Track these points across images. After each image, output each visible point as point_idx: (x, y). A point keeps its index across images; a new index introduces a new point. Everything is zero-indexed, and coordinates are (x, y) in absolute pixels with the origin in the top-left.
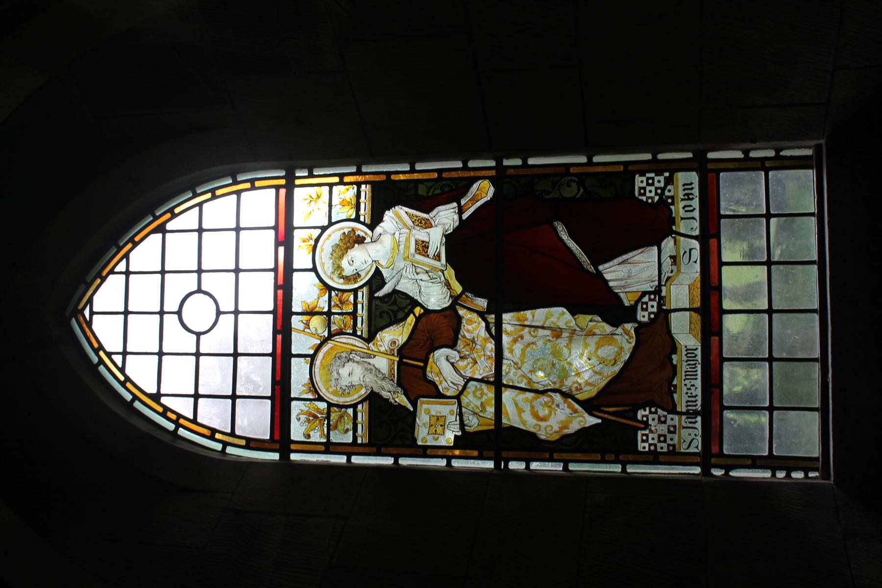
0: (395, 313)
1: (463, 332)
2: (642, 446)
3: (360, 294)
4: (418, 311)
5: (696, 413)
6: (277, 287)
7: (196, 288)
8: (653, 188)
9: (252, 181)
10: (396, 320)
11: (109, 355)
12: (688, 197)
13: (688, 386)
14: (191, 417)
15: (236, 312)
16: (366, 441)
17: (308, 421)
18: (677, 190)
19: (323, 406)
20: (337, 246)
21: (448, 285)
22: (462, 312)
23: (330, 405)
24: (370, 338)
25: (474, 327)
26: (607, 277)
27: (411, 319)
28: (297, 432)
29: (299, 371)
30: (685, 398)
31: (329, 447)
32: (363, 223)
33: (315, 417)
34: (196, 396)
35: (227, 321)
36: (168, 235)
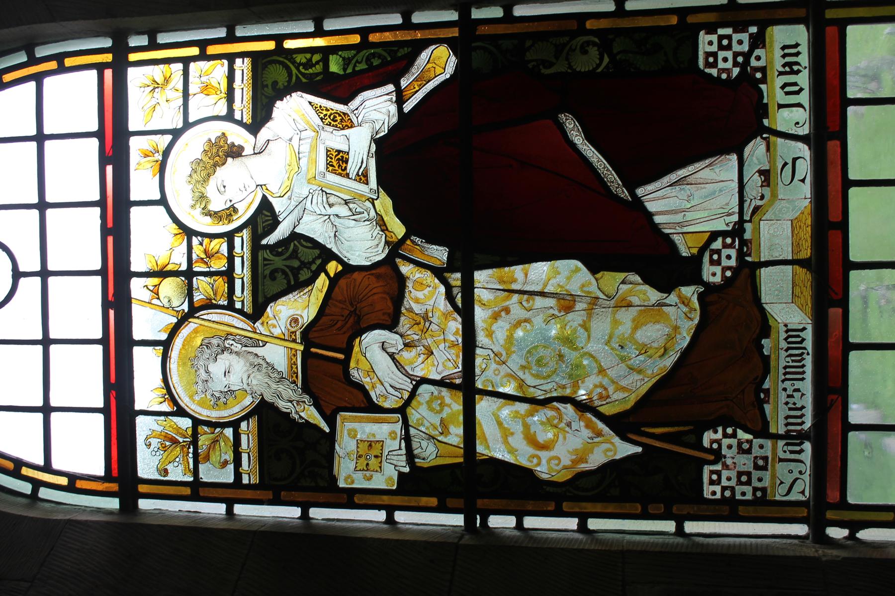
0: (296, 272)
1: (409, 302)
2: (709, 491)
3: (237, 241)
4: (333, 267)
5: (802, 436)
6: (105, 231)
8: (729, 54)
9: (60, 58)
10: (297, 283)
12: (791, 68)
13: (789, 392)
15: (44, 274)
16: (255, 480)
17: (165, 448)
18: (771, 57)
19: (185, 423)
20: (199, 161)
21: (381, 224)
22: (406, 269)
23: (197, 422)
24: (256, 314)
25: (425, 294)
26: (651, 207)
27: (322, 282)
28: (147, 465)
29: (146, 364)
30: (783, 411)
31: (197, 490)
32: (240, 123)
33: (174, 442)
35: (30, 287)
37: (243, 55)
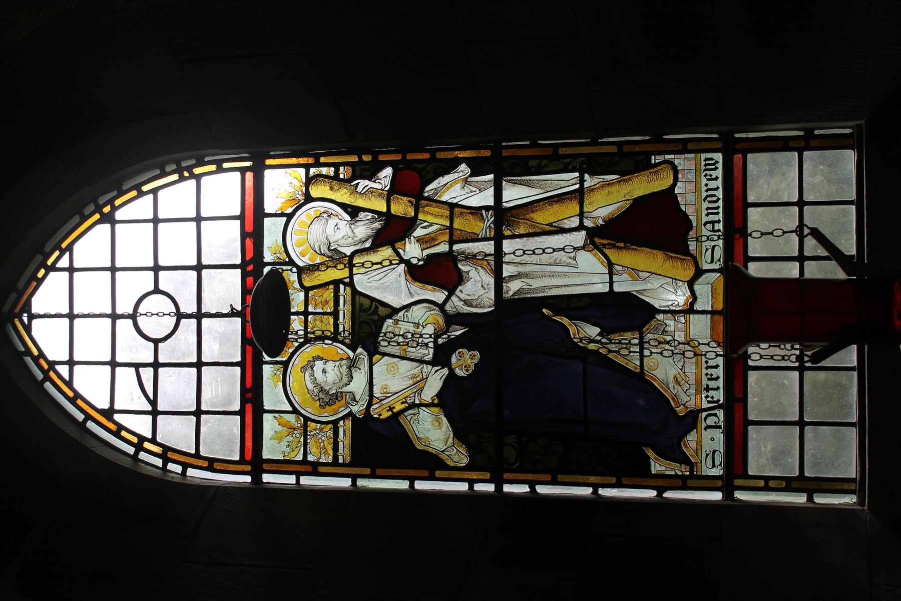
7: (152, 288)
11: (52, 364)
36: (118, 226)
37: (344, 164)
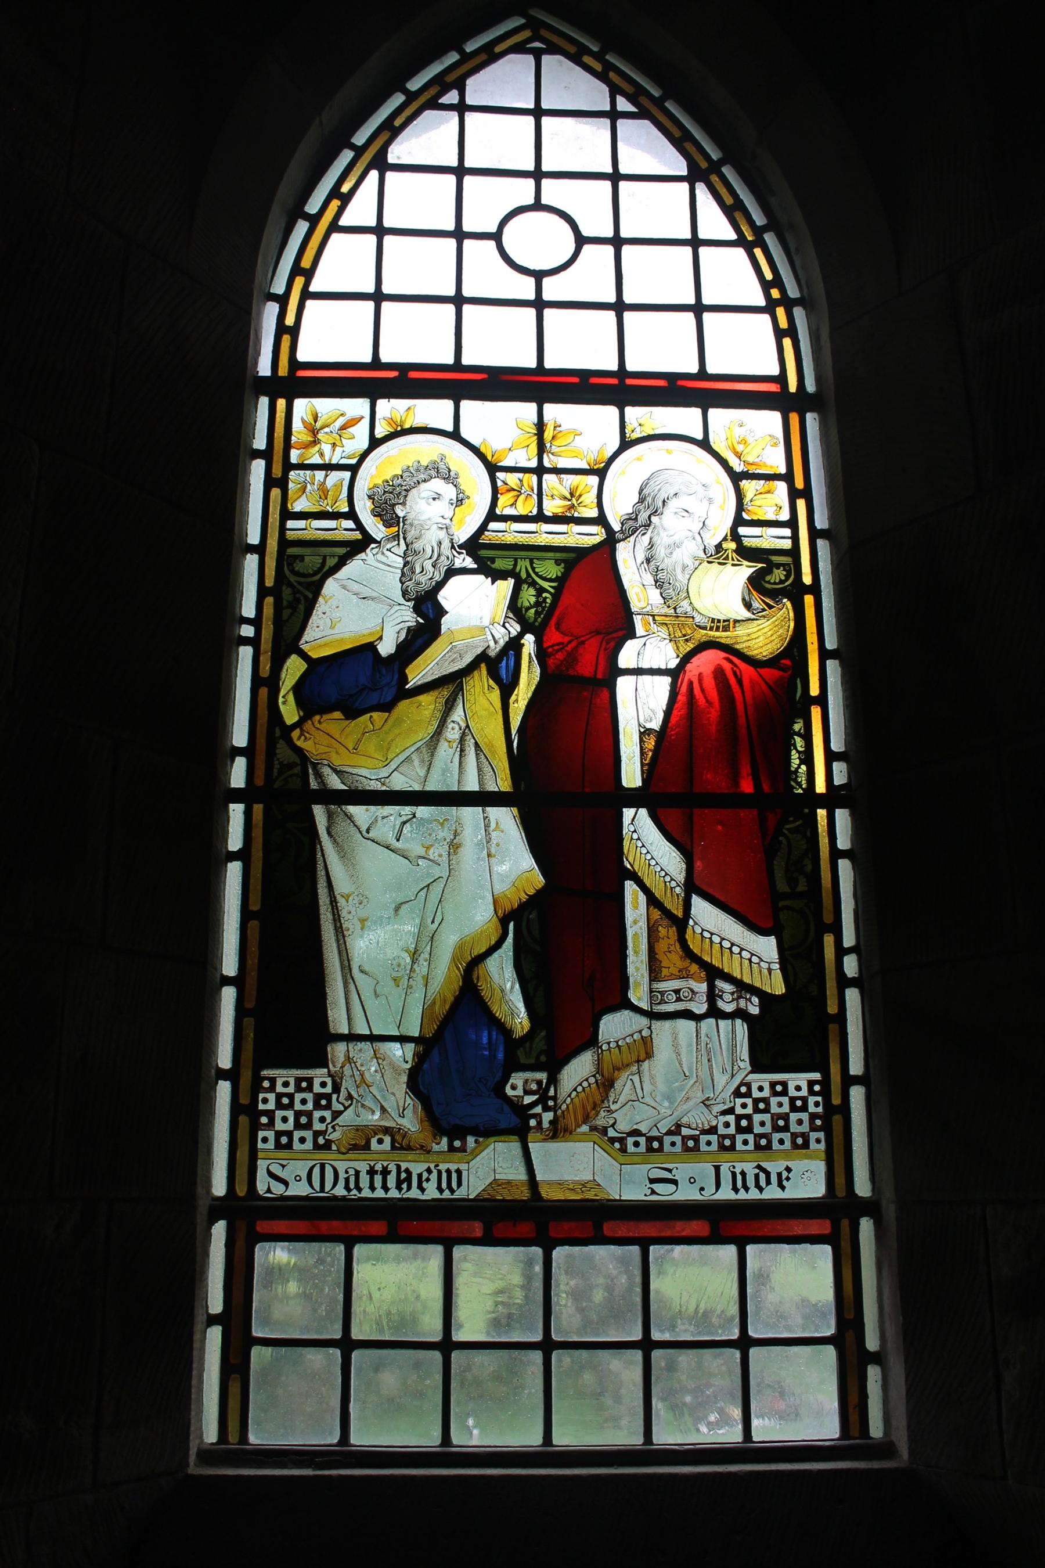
9: (792, 332)
14: (343, 222)
34: (380, 231)
36: (685, 186)
